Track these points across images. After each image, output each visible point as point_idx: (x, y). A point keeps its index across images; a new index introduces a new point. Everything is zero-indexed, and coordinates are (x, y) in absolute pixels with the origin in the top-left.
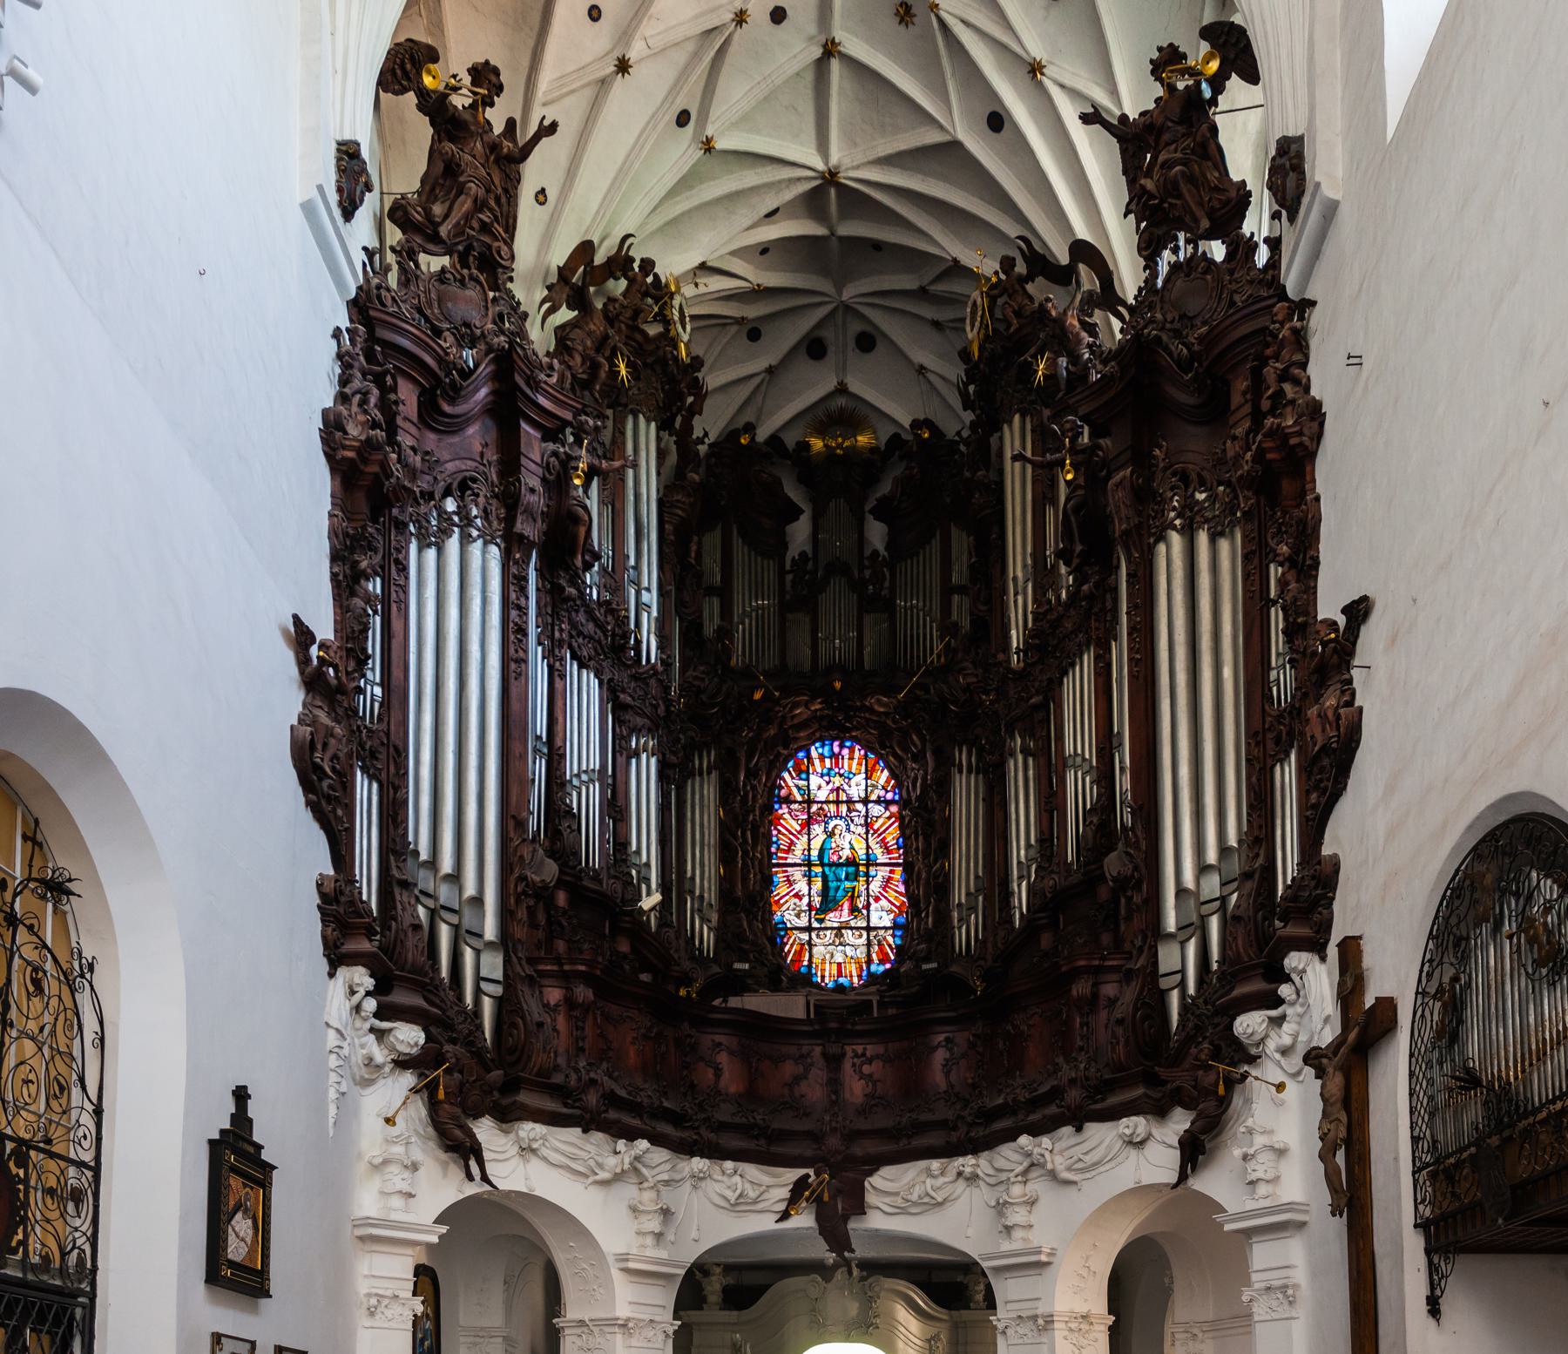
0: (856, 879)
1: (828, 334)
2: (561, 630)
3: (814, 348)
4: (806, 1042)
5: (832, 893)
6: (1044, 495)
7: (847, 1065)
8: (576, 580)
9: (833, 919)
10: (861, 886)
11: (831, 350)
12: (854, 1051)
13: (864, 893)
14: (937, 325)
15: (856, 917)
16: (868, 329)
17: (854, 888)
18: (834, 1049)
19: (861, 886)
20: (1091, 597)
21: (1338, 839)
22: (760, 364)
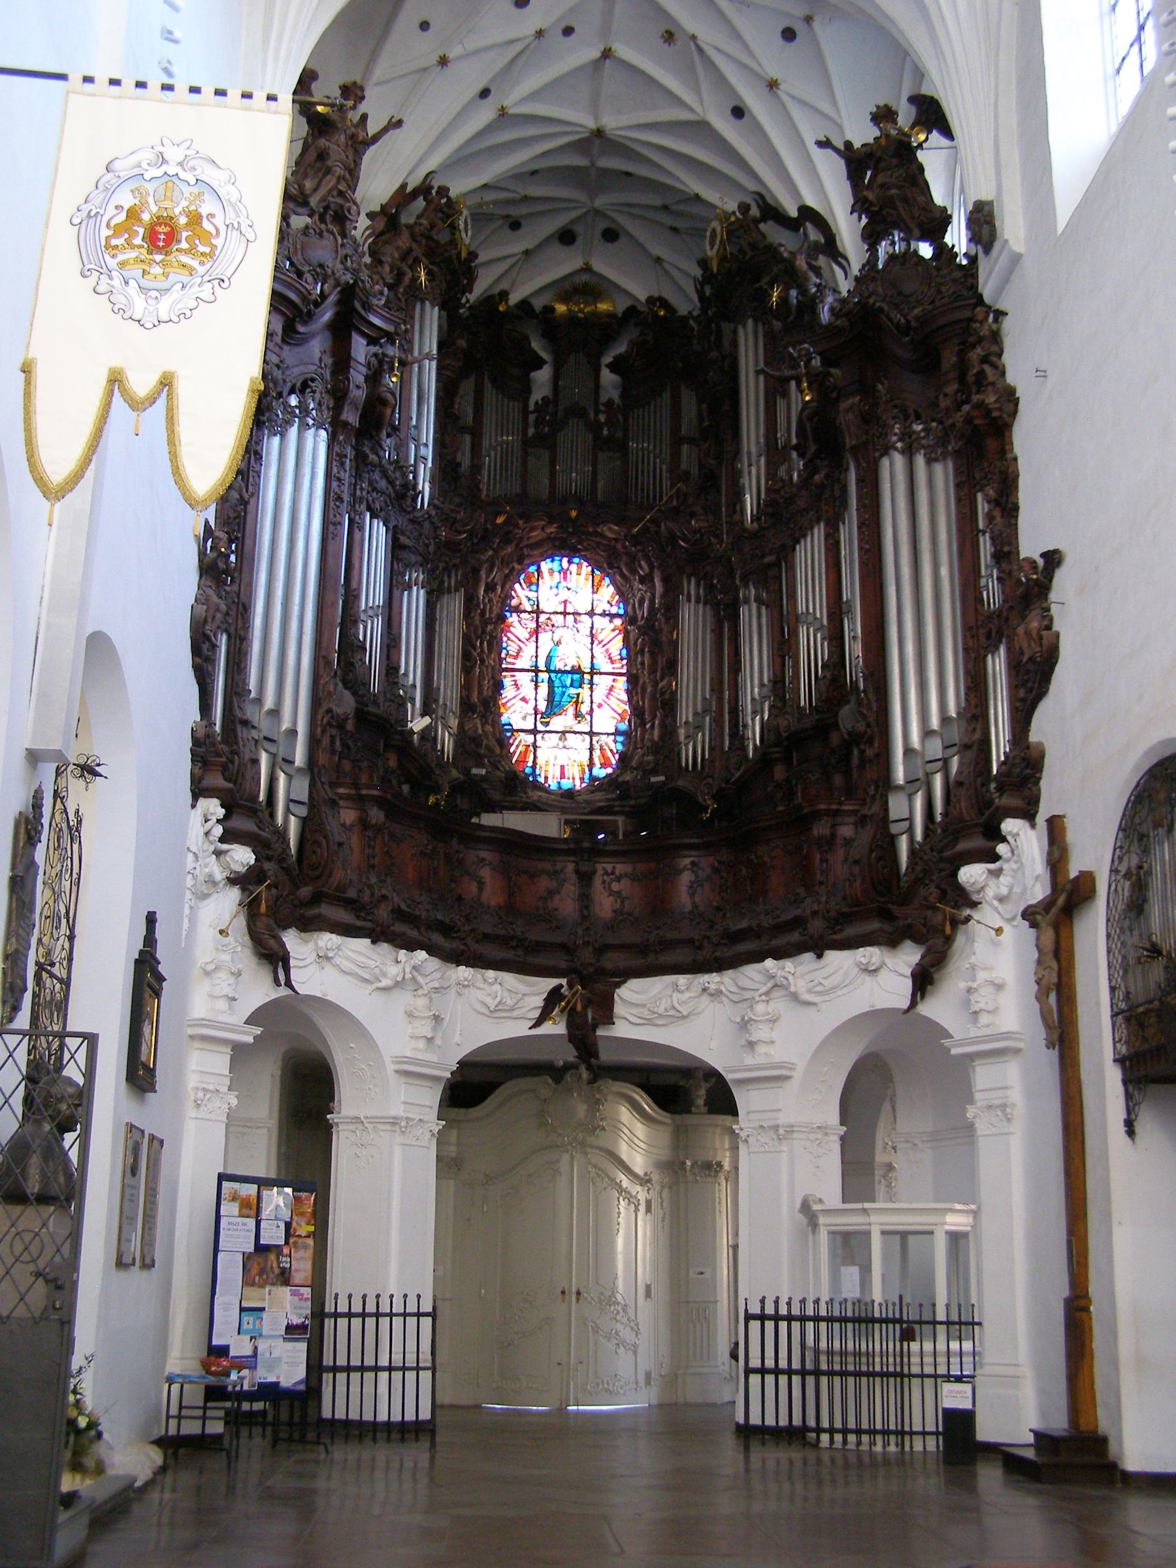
0: (580, 687)
1: (579, 229)
2: (362, 489)
3: (566, 237)
4: (560, 858)
5: (557, 698)
6: (776, 390)
8: (377, 447)
9: (557, 723)
10: (585, 692)
11: (579, 242)
12: (604, 869)
14: (674, 229)
16: (613, 226)
17: (578, 695)
18: (585, 868)
19: (585, 692)
20: (822, 486)
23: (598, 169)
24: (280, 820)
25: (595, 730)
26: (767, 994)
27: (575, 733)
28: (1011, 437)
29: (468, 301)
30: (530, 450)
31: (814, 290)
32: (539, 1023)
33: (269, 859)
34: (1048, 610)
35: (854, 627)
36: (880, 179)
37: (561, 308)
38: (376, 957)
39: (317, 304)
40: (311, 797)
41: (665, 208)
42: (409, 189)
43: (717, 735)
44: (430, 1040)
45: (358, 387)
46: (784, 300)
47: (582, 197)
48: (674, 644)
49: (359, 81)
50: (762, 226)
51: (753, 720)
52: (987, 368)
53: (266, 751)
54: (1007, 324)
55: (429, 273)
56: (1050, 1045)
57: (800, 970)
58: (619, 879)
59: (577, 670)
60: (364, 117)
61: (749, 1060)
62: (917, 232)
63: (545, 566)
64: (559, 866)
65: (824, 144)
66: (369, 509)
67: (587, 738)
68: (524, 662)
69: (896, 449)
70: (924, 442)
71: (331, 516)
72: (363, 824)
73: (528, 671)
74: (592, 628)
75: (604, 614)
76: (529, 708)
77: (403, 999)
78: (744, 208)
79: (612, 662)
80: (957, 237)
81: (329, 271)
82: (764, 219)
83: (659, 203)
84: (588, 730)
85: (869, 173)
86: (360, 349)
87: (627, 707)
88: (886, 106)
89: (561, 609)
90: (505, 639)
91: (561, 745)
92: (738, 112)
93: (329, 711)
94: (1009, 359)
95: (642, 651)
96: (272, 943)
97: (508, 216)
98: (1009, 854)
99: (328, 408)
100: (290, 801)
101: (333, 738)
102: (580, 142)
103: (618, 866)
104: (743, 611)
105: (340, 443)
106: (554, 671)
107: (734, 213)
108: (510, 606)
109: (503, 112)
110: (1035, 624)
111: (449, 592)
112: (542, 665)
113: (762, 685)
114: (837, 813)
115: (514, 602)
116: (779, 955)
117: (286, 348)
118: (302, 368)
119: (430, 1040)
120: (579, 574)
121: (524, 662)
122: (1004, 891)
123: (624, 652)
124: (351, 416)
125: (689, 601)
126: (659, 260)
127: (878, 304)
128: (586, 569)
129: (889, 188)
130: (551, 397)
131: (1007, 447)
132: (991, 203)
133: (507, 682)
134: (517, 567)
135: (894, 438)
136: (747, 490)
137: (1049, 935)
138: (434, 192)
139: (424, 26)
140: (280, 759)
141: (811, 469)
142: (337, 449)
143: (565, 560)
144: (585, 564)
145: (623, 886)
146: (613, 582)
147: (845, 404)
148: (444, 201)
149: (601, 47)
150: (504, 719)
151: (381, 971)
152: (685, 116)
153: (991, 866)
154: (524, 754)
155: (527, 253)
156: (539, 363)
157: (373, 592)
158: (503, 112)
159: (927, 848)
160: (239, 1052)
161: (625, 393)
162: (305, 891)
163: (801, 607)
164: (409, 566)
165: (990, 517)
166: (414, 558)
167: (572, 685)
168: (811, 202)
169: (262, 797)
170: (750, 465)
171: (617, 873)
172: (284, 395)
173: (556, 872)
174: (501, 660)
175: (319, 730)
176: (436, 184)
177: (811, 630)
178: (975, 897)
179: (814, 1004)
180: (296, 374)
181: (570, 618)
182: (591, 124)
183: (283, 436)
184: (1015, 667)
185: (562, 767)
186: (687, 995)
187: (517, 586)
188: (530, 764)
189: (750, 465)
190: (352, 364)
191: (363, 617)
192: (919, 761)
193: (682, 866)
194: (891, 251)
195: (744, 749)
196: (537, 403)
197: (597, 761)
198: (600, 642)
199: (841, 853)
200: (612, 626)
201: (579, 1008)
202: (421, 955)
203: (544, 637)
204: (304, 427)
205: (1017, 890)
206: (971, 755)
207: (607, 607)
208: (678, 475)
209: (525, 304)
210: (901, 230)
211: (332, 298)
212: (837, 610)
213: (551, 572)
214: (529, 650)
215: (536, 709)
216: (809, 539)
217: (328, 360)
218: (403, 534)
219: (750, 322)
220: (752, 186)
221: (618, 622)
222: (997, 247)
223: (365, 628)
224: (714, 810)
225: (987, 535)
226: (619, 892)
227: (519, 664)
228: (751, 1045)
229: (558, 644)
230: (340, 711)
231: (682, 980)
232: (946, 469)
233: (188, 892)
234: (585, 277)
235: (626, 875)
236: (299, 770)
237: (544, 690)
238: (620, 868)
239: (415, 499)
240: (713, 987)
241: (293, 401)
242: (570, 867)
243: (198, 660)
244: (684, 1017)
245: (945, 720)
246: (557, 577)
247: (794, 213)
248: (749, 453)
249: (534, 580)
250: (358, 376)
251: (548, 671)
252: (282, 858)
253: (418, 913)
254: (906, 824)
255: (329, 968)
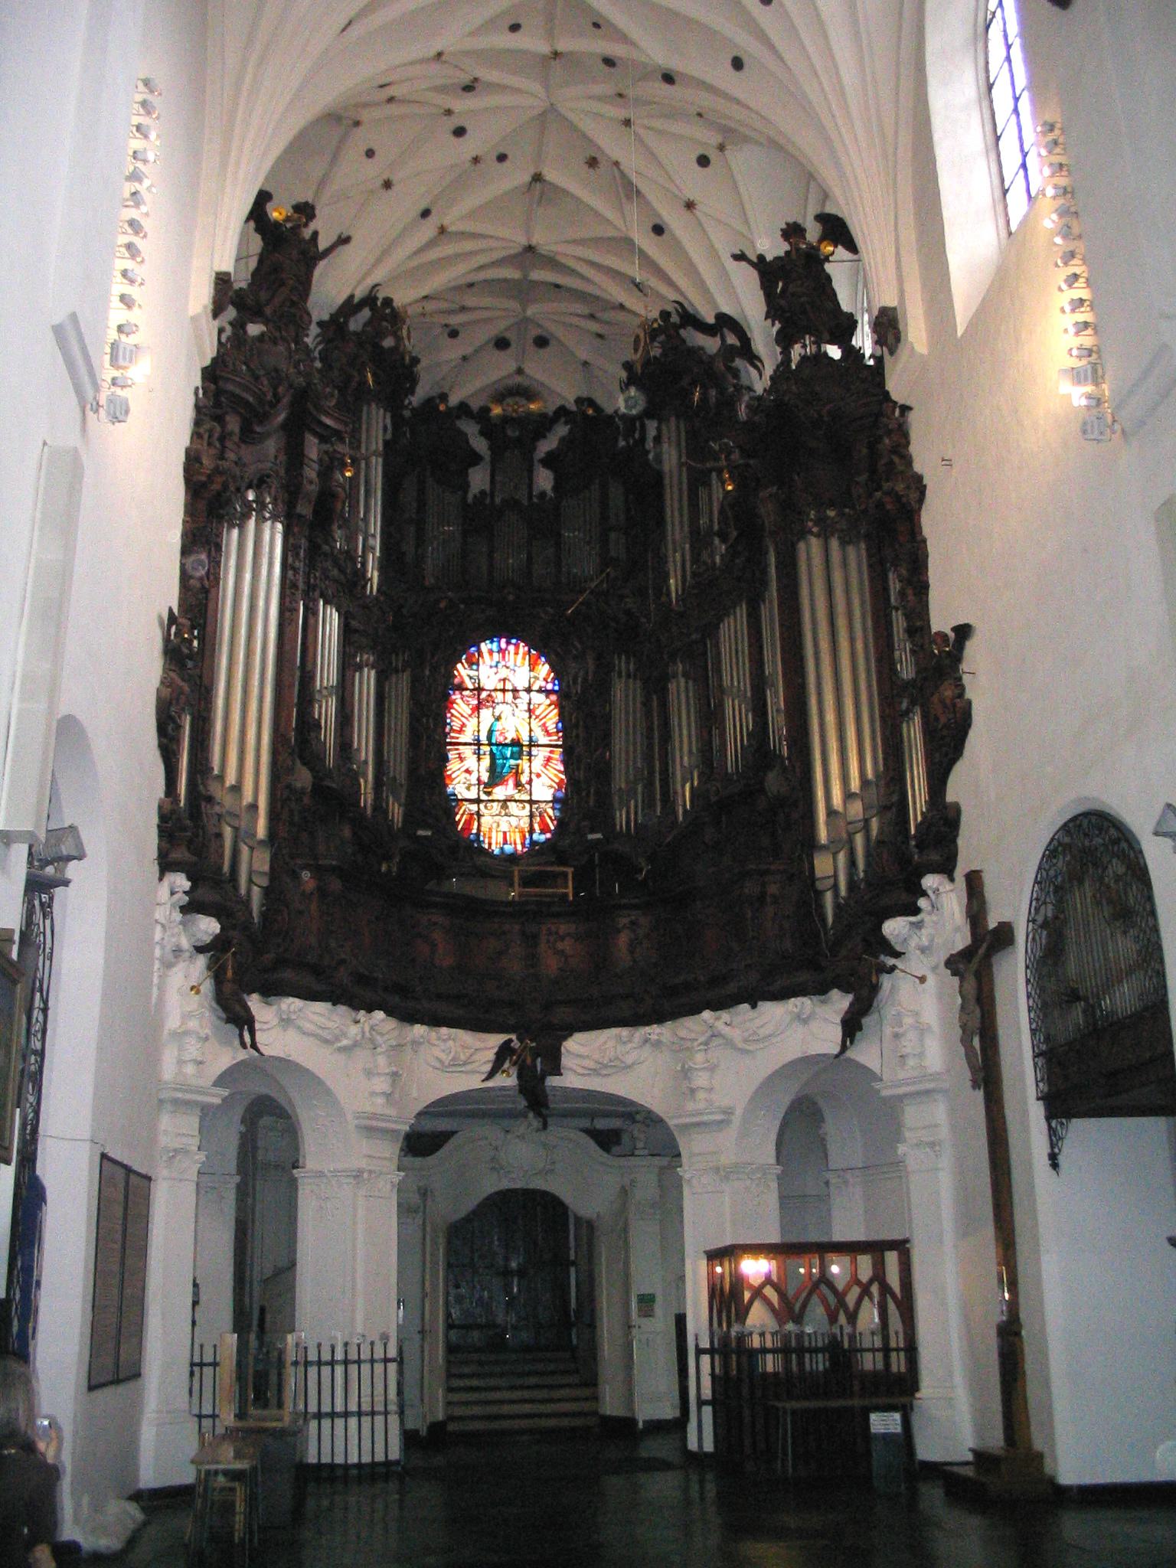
0: (518, 756)
2: (315, 578)
3: (502, 344)
5: (499, 770)
7: (543, 938)
8: (329, 538)
9: (500, 792)
10: (524, 764)
12: (549, 929)
13: (527, 771)
14: (600, 336)
15: (520, 791)
16: (544, 334)
17: (518, 766)
19: (524, 764)
21: (953, 793)
22: (461, 352)
23: (530, 281)
24: (243, 891)
25: (534, 798)
26: (706, 1043)
27: (516, 801)
28: (919, 522)
29: (410, 403)
30: (470, 540)
31: (732, 389)
32: (491, 1075)
33: (234, 927)
34: (960, 679)
35: (776, 700)
36: (792, 288)
37: (497, 411)
38: (336, 1018)
39: (273, 405)
40: (272, 868)
41: (592, 316)
42: (356, 300)
43: (649, 803)
44: (388, 1096)
45: (311, 482)
46: (704, 398)
47: (513, 305)
48: (608, 719)
49: (310, 201)
50: (682, 332)
51: (683, 787)
52: (896, 459)
53: (230, 826)
54: (912, 417)
55: (374, 375)
56: (975, 1085)
57: (737, 1020)
58: (562, 939)
59: (516, 743)
60: (315, 234)
61: (690, 1106)
62: (826, 336)
63: (485, 647)
64: (506, 927)
65: (740, 257)
66: (322, 595)
67: (527, 806)
68: (467, 737)
69: (812, 533)
70: (838, 526)
71: (287, 604)
72: (322, 892)
73: (470, 744)
74: (529, 704)
75: (540, 691)
76: (473, 779)
77: (362, 1057)
78: (665, 315)
79: (548, 734)
80: (864, 340)
81: (284, 375)
82: (683, 326)
83: (587, 311)
84: (528, 798)
85: (780, 284)
86: (313, 448)
87: (563, 777)
88: (795, 223)
89: (500, 686)
90: (449, 715)
91: (503, 813)
92: (658, 230)
93: (289, 787)
94: (915, 449)
95: (577, 726)
96: (238, 1008)
97: (446, 325)
98: (930, 908)
99: (283, 501)
100: (250, 873)
101: (291, 811)
102: (515, 256)
103: (562, 926)
104: (672, 686)
105: (294, 535)
106: (498, 745)
107: (656, 320)
108: (453, 684)
109: (442, 230)
110: (948, 693)
111: (397, 671)
112: (483, 739)
113: (690, 752)
114: (763, 873)
115: (456, 681)
116: (717, 1006)
117: (243, 446)
118: (260, 465)
119: (388, 1096)
120: (516, 653)
121: (467, 737)
122: (925, 942)
123: (560, 725)
124: (305, 509)
125: (620, 676)
126: (585, 364)
127: (792, 402)
128: (523, 648)
129: (800, 297)
130: (488, 490)
131: (916, 530)
132: (895, 309)
133: (452, 755)
134: (459, 648)
135: (810, 524)
136: (672, 573)
137: (971, 983)
138: (379, 303)
139: (370, 153)
140: (242, 833)
141: (733, 553)
142: (291, 541)
143: (503, 641)
144: (522, 644)
145: (566, 945)
146: (548, 661)
147: (763, 494)
148: (388, 311)
149: (532, 171)
150: (450, 790)
151: (341, 1030)
152: (612, 233)
153: (912, 919)
154: (469, 823)
155: (464, 358)
156: (475, 458)
157: (327, 672)
158: (442, 230)
159: (852, 903)
160: (206, 1112)
161: (555, 488)
162: (269, 957)
163: (726, 681)
164: (361, 649)
165: (902, 594)
166: (364, 641)
167: (512, 757)
168: (726, 309)
169: (226, 868)
170: (675, 551)
171: (561, 932)
172: (243, 489)
173: (504, 933)
174: (446, 735)
175: (279, 806)
176: (381, 295)
177: (736, 702)
178: (898, 948)
179: (747, 1052)
180: (252, 471)
181: (509, 695)
182: (524, 242)
183: (242, 528)
184: (929, 733)
185: (505, 833)
186: (630, 1045)
187: (459, 666)
188: (474, 831)
189: (675, 551)
190: (306, 461)
191: (317, 697)
192: (842, 824)
193: (620, 926)
194: (803, 352)
195: (675, 813)
196: (475, 496)
197: (536, 827)
198: (537, 717)
199: (770, 910)
200: (548, 702)
201: (529, 1061)
202: (380, 1015)
203: (486, 714)
204: (261, 520)
205: (938, 940)
206: (890, 815)
207: (543, 684)
208: (606, 561)
209: (463, 409)
210: (811, 335)
211: (286, 400)
212: (760, 684)
213: (491, 652)
214: (471, 725)
215: (479, 779)
216: (732, 617)
217: (282, 458)
218: (354, 618)
219: (673, 419)
220: (673, 296)
221: (554, 697)
222: (901, 346)
223: (320, 707)
224: (648, 871)
225: (900, 612)
226: (563, 951)
227: (463, 739)
228: (693, 1091)
229: (498, 719)
230: (299, 785)
231: (624, 1032)
232: (858, 550)
233: (157, 962)
234: (519, 379)
235: (569, 934)
236: (261, 842)
237: (486, 762)
238: (563, 928)
239: (364, 587)
240: (654, 1037)
241: (251, 496)
242: (517, 927)
243: (165, 741)
244: (629, 1067)
245: (865, 782)
246: (496, 656)
247: (711, 320)
248: (674, 542)
249: (474, 660)
250: (311, 473)
251: (490, 744)
252: (246, 926)
253: (375, 975)
254: (832, 881)
255: (292, 1034)
